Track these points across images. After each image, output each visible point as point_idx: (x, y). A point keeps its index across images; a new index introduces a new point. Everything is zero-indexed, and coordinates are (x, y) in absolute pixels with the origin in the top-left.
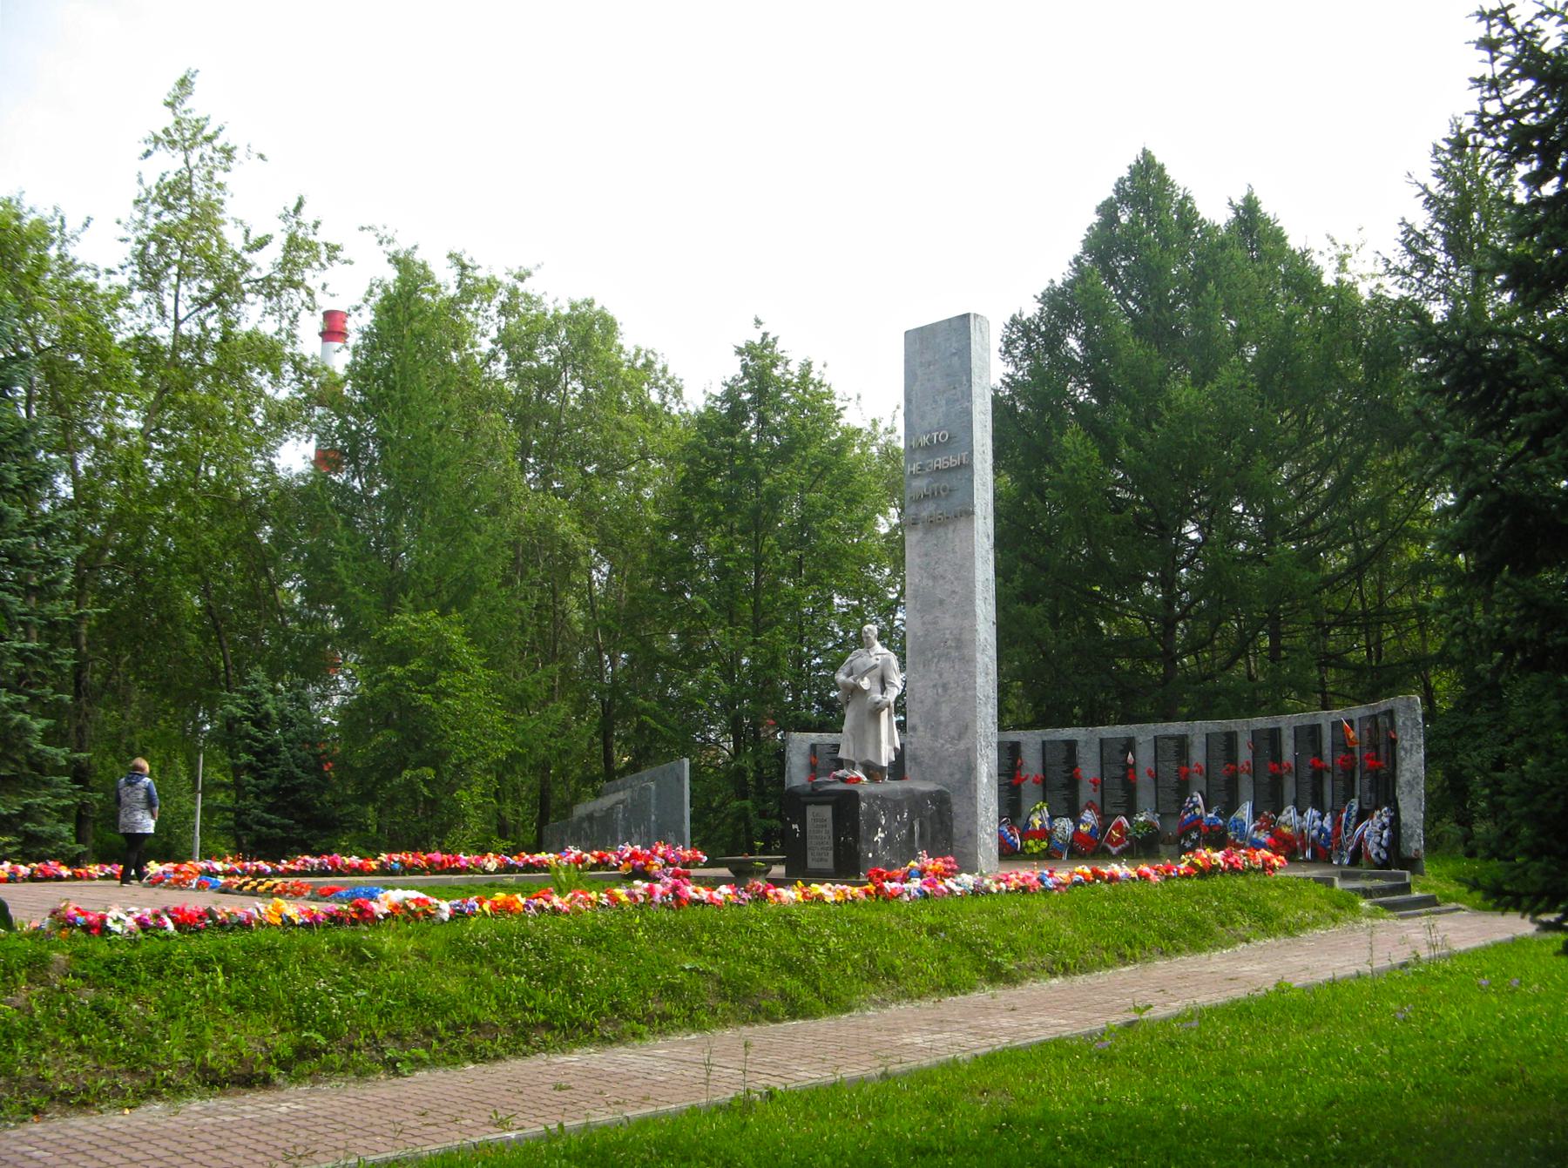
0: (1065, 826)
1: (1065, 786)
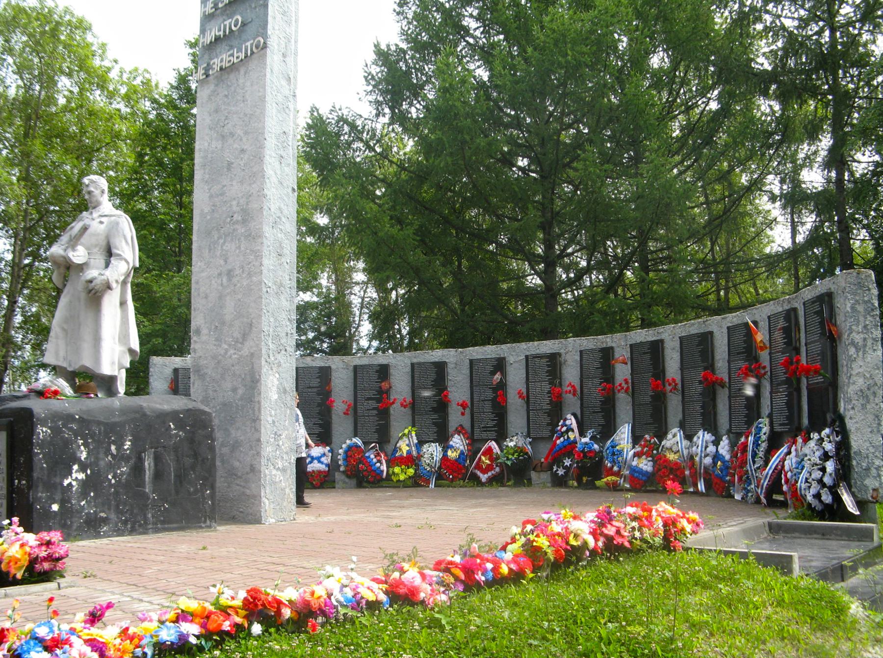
0: (433, 452)
1: (434, 410)
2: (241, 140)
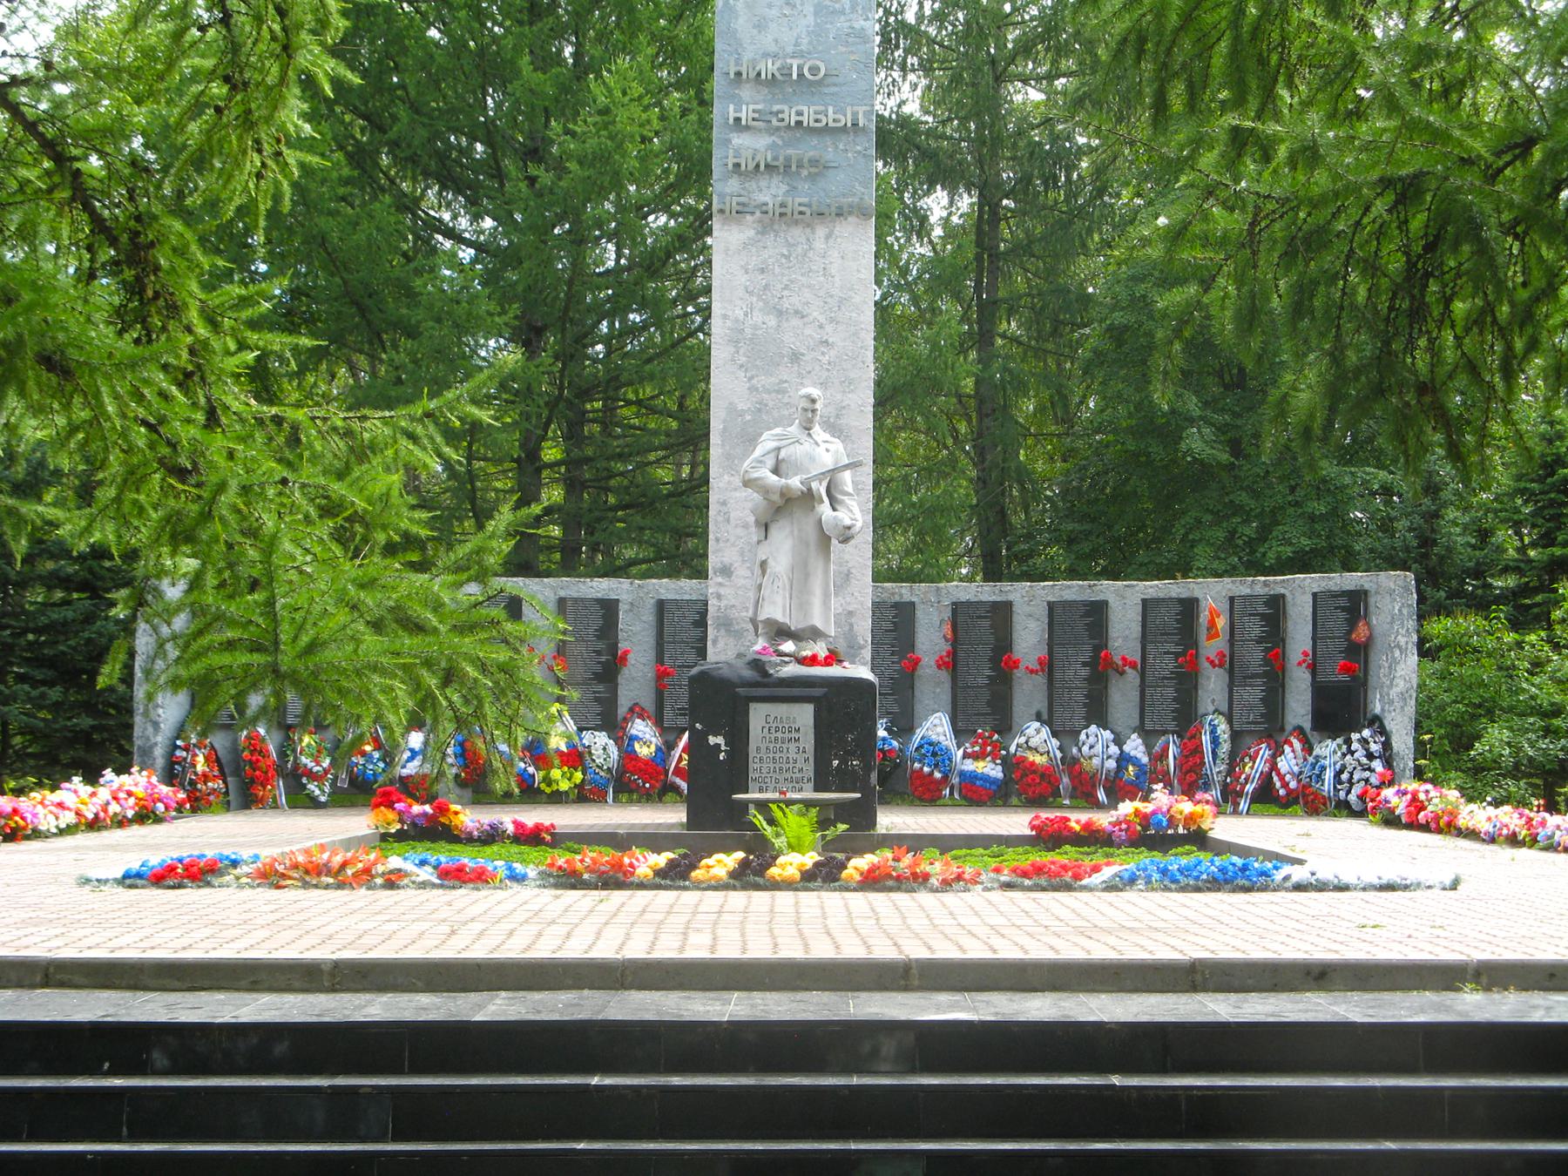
0: (600, 744)
2: (821, 327)
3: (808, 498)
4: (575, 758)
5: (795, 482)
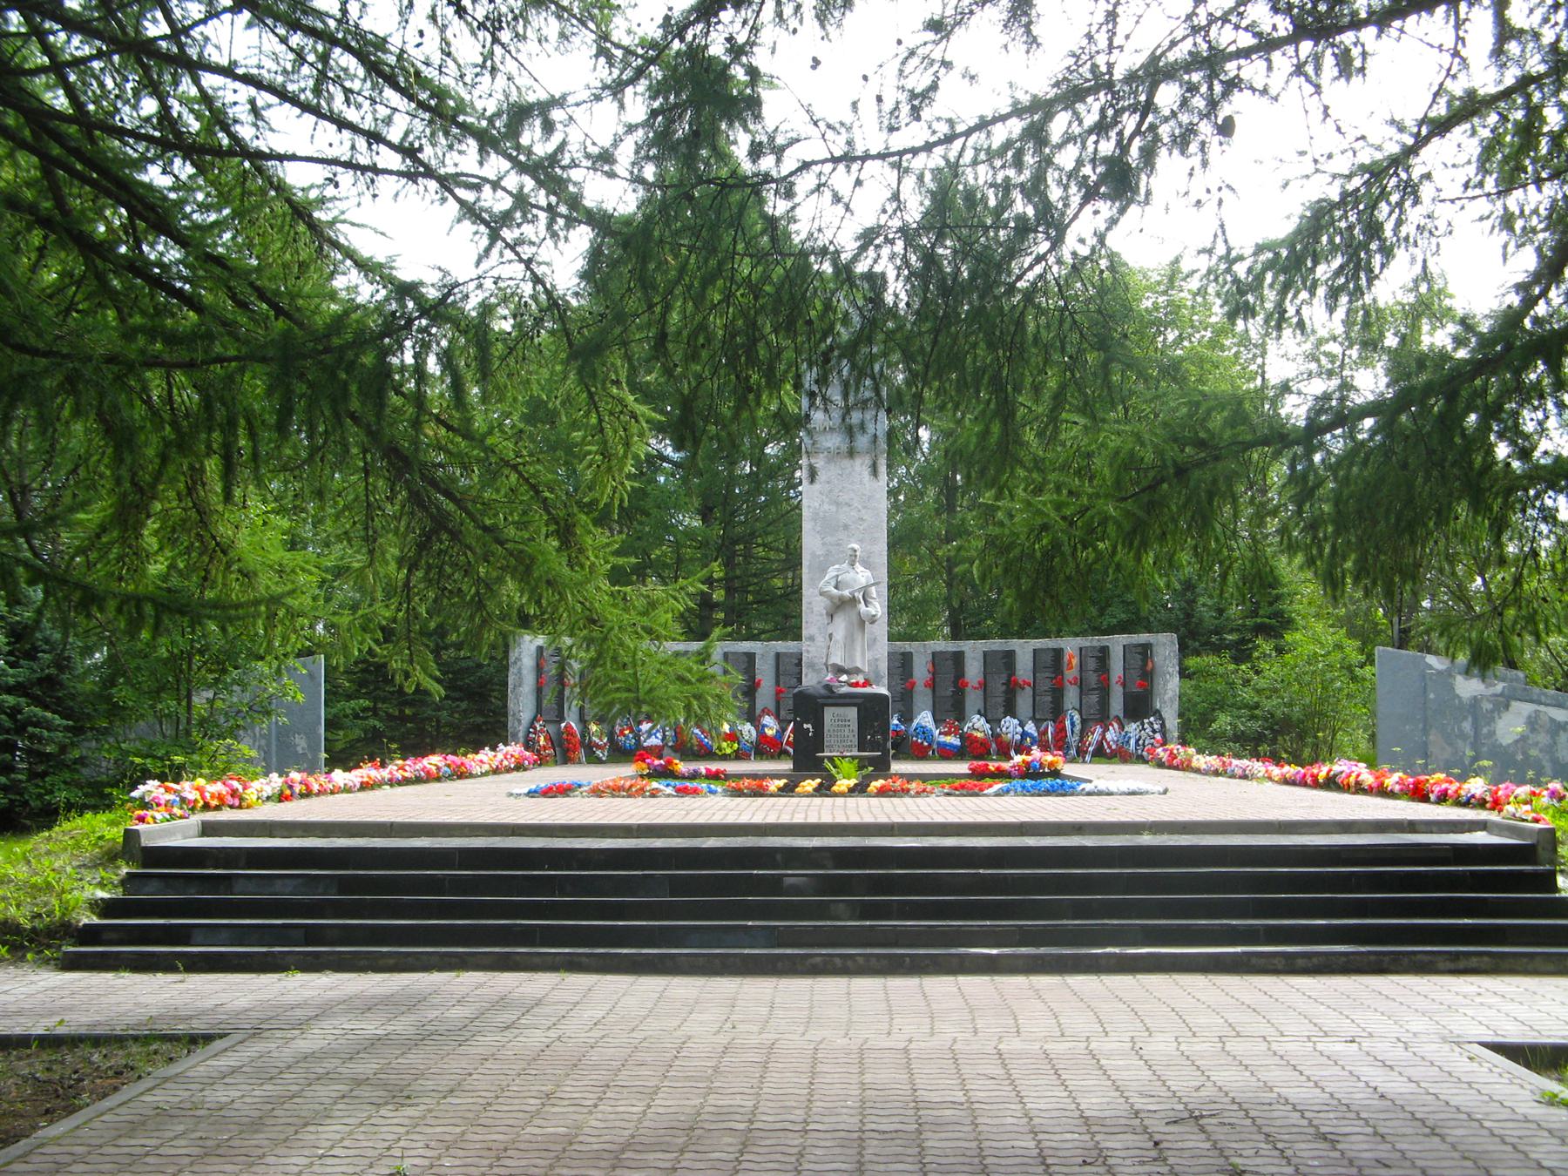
0: (748, 731)
3: (853, 601)
4: (732, 737)
5: (846, 593)
